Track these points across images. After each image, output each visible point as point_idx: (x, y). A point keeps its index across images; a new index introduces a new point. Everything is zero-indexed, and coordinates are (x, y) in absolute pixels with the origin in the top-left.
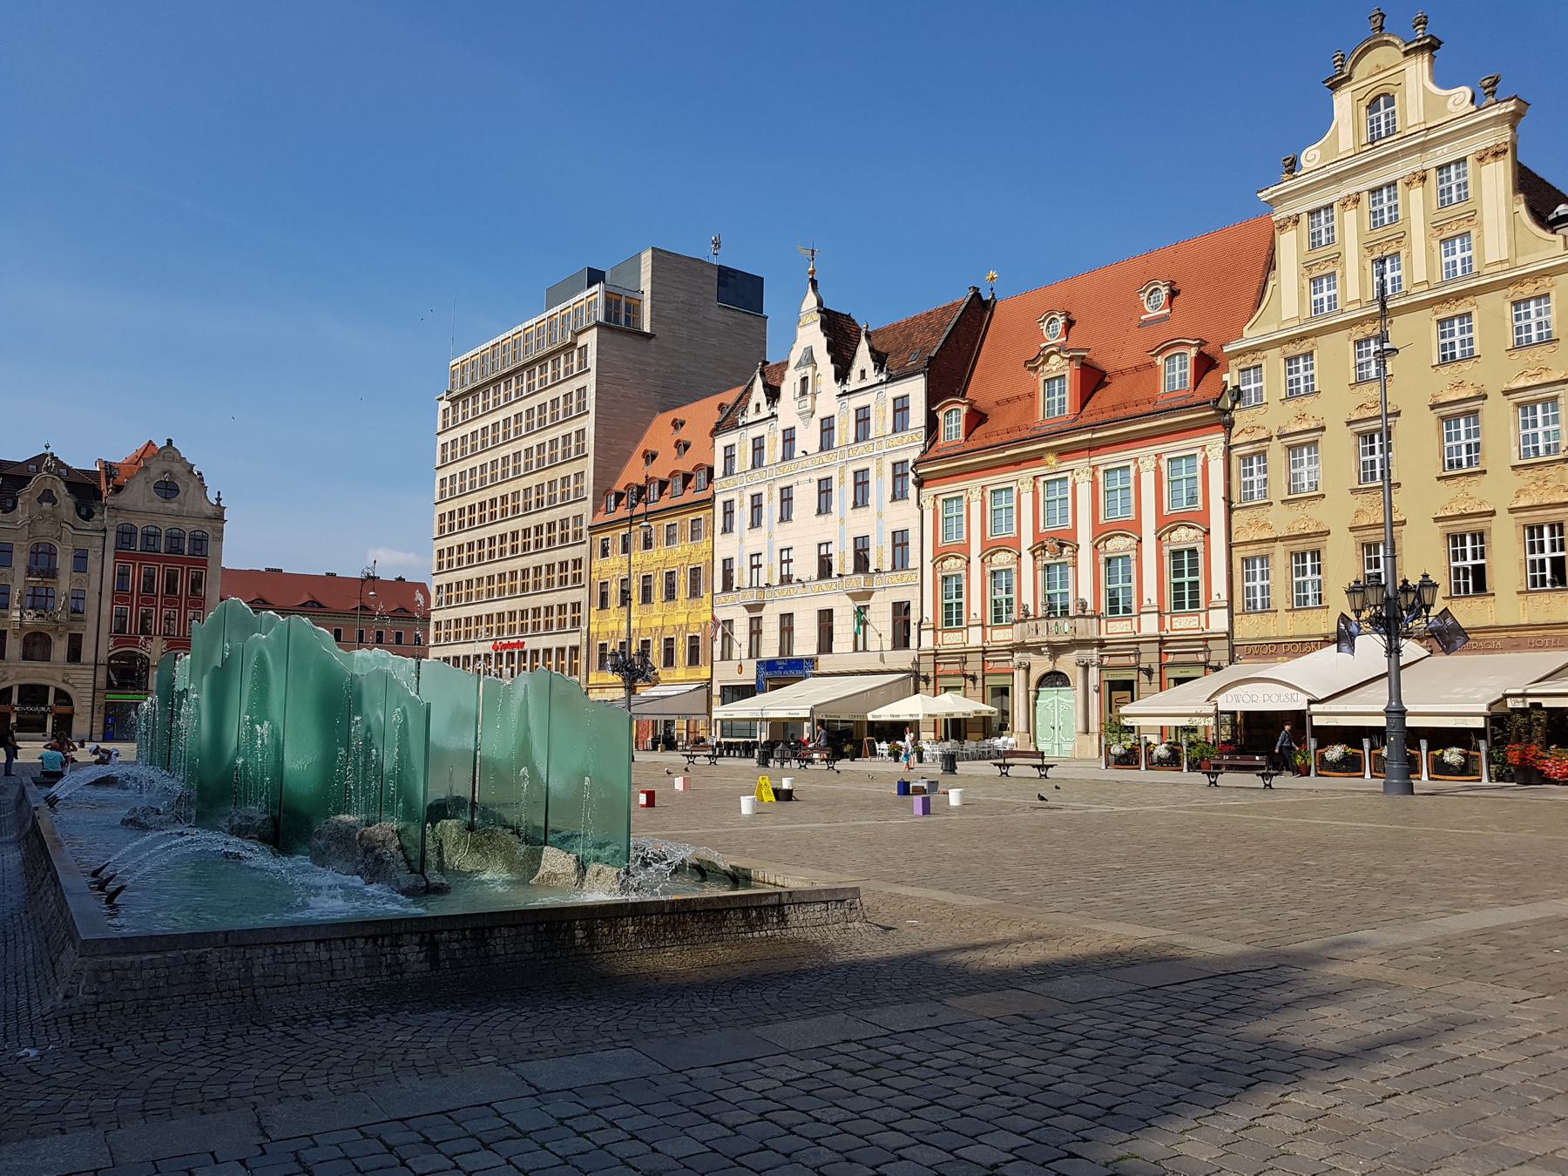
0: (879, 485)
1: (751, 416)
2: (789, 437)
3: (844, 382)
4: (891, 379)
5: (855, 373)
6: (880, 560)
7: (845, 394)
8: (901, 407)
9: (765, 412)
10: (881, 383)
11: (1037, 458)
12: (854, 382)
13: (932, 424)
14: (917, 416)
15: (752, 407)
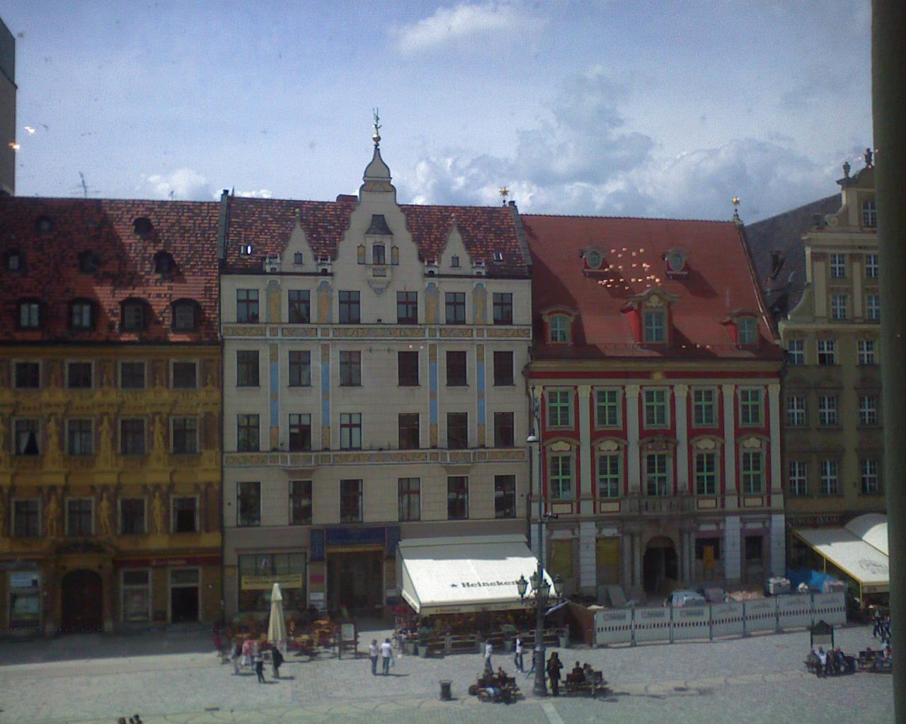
0: (480, 368)
1: (287, 262)
2: (350, 301)
3: (431, 263)
4: (490, 276)
5: (446, 258)
6: (481, 435)
7: (431, 274)
8: (504, 303)
9: (310, 264)
10: (479, 276)
11: (646, 375)
12: (444, 265)
13: (539, 326)
14: (522, 311)
15: (289, 255)
